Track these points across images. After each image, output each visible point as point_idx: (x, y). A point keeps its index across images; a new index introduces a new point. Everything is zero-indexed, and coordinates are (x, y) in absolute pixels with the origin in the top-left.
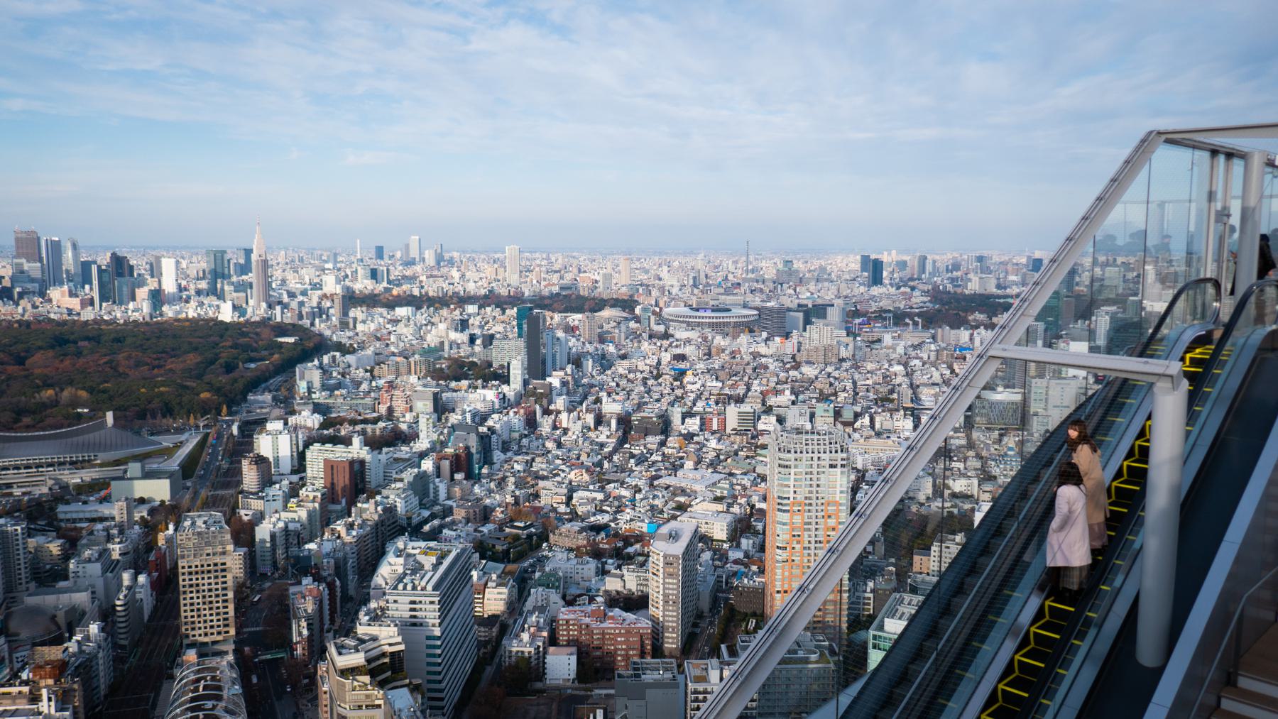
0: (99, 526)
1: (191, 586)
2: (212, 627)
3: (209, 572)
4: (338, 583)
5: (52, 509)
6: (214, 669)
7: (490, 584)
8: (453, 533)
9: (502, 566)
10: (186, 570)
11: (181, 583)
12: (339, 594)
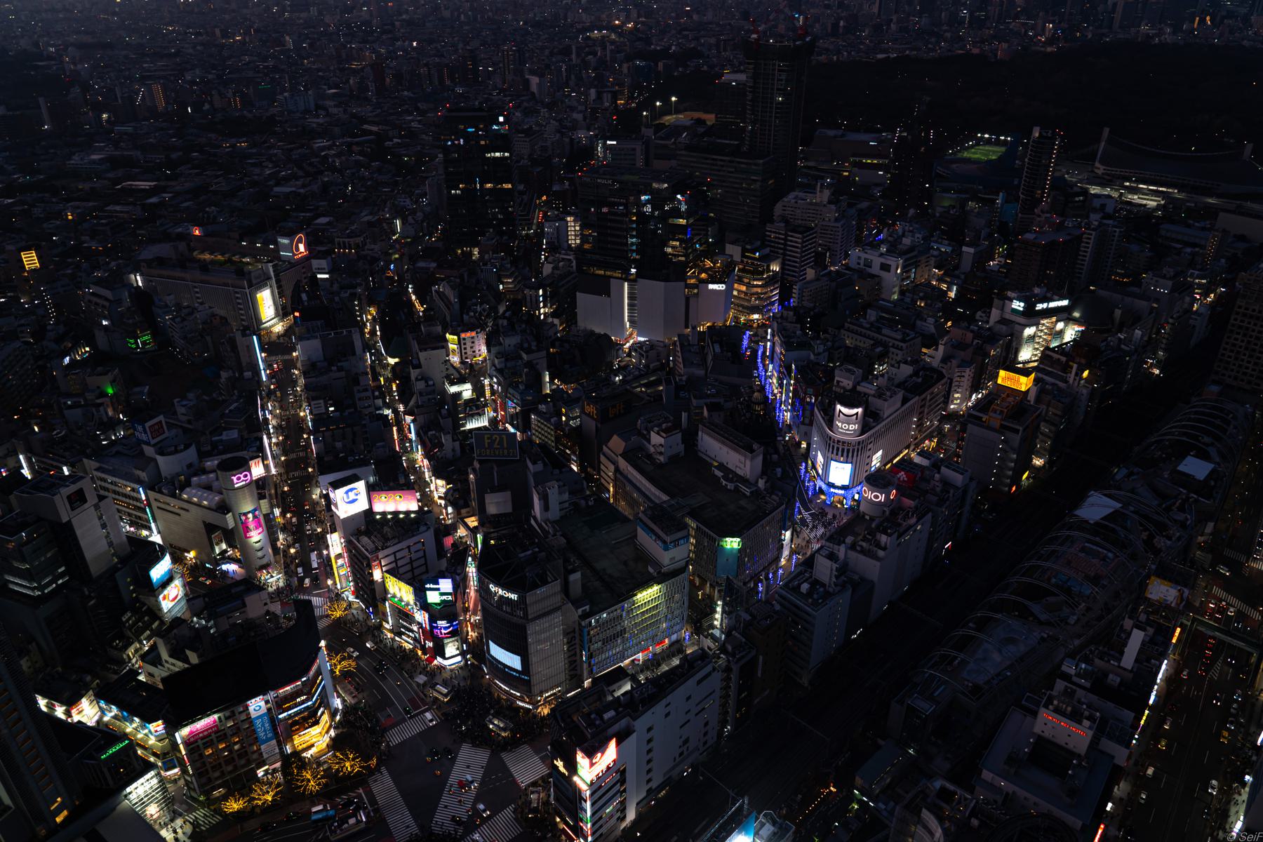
0: (1189, 250)
1: (1240, 327)
2: (1245, 374)
10: (1242, 310)
11: (1232, 321)
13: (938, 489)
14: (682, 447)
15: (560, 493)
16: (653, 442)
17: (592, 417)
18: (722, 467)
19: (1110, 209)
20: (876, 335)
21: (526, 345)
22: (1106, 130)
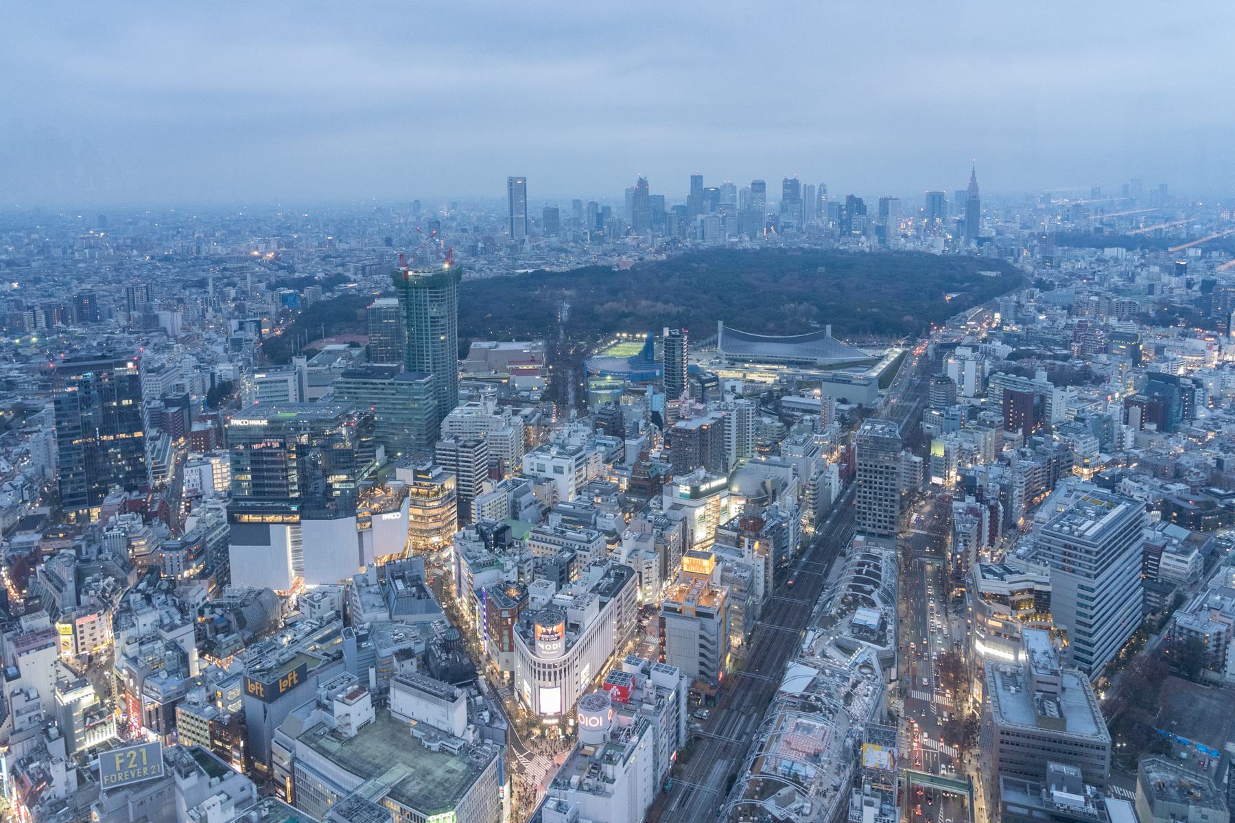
0: (808, 417)
3: (881, 473)
4: (1001, 508)
5: (779, 397)
6: (876, 558)
7: (1168, 548)
8: (1136, 485)
9: (1188, 532)
12: (1001, 519)
13: (653, 697)
14: (370, 713)
15: (223, 811)
16: (337, 713)
17: (258, 697)
18: (422, 725)
19: (739, 390)
20: (561, 540)
21: (167, 621)
22: (720, 323)
